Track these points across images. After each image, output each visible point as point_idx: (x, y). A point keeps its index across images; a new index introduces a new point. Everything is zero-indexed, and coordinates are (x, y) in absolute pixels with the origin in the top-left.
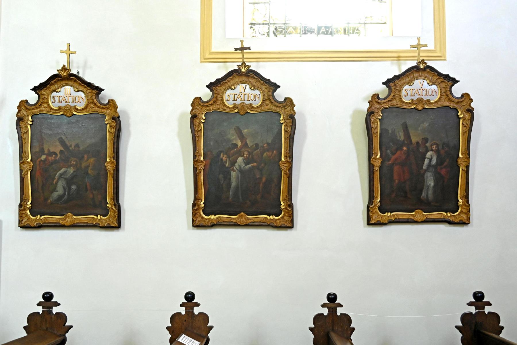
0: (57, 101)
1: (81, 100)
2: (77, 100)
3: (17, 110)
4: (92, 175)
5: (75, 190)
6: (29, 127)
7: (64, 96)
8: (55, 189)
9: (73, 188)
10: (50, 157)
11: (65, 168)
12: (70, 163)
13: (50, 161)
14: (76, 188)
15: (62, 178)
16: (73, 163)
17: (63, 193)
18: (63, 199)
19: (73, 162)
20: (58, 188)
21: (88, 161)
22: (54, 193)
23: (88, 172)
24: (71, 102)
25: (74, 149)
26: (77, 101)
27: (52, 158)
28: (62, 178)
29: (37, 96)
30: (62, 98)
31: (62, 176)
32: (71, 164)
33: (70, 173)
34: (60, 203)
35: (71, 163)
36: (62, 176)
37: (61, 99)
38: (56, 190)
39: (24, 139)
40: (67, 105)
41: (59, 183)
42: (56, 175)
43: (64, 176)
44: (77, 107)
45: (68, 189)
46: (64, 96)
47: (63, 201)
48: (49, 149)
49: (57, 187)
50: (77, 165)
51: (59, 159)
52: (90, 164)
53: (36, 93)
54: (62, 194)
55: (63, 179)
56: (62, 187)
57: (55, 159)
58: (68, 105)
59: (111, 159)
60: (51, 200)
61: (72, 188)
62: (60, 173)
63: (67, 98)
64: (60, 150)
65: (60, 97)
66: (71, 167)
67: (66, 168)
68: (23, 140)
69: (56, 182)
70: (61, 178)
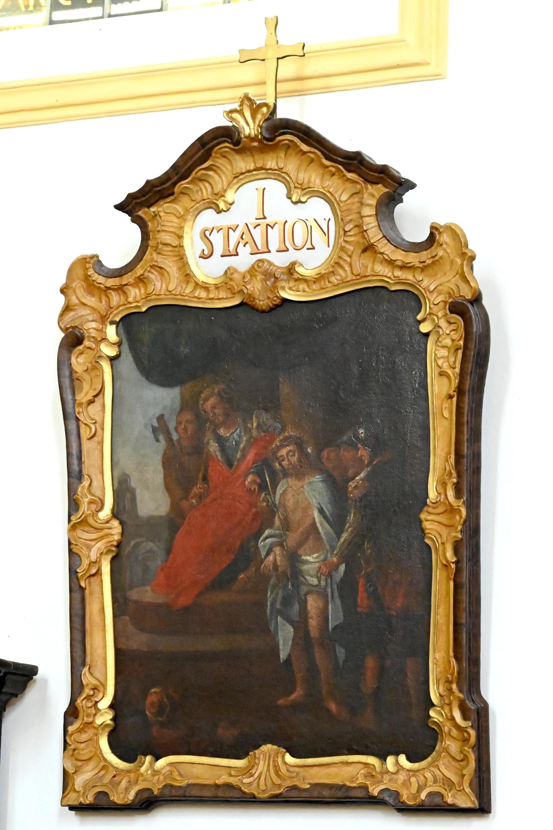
2: (300, 238)
24: (276, 248)
26: (299, 242)
30: (239, 231)
37: (234, 237)
63: (257, 234)
65: (230, 230)
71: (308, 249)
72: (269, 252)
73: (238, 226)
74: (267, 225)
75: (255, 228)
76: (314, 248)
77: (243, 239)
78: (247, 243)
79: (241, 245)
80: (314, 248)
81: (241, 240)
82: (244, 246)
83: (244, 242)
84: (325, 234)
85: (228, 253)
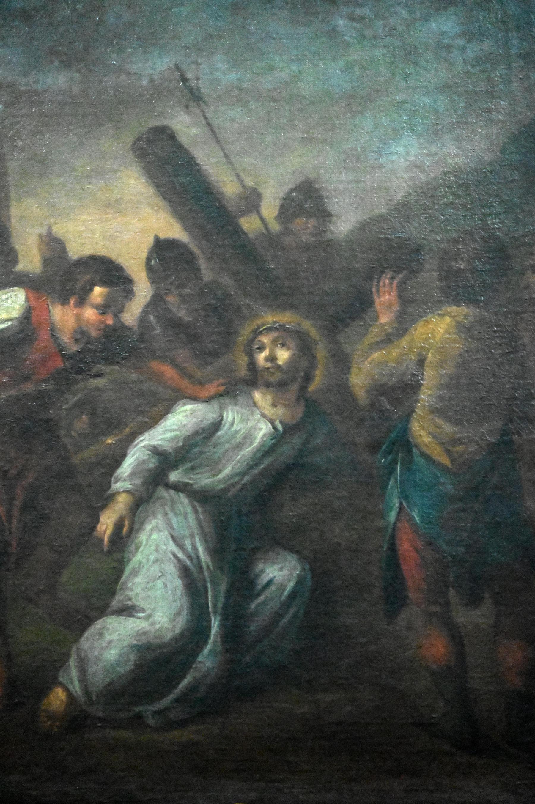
4: (446, 461)
5: (293, 595)
8: (113, 593)
9: (270, 582)
10: (64, 302)
11: (194, 399)
12: (243, 361)
13: (65, 338)
14: (300, 582)
15: (177, 487)
16: (272, 358)
17: (182, 621)
18: (185, 683)
19: (275, 342)
20: (138, 580)
21: (404, 342)
22: (99, 624)
23: (406, 430)
27: (78, 317)
28: (177, 487)
31: (174, 476)
32: (252, 365)
33: (239, 446)
34: (151, 722)
35: (251, 354)
36: (174, 476)
38: (115, 604)
41: (143, 537)
42: (118, 461)
43: (193, 469)
45: (223, 588)
47: (177, 700)
48: (58, 230)
49: (127, 572)
50: (308, 378)
51: (142, 320)
52: (421, 362)
54: (169, 636)
55: (183, 498)
56: (171, 569)
57: (110, 322)
60: (76, 688)
61: (265, 579)
62: (155, 451)
64: (151, 240)
66: (257, 396)
67: (207, 400)
69: (119, 526)
70: (162, 492)
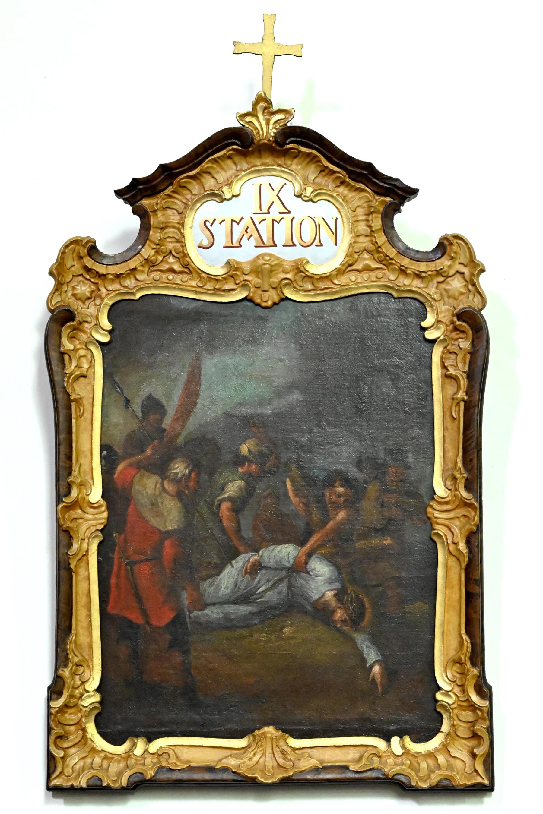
0: (221, 239)
1: (325, 233)
2: (308, 235)
3: (51, 283)
6: (98, 354)
7: (255, 217)
25: (180, 441)
29: (136, 221)
37: (238, 230)
39: (75, 400)
40: (263, 255)
44: (313, 269)
46: (255, 217)
53: (134, 212)
58: (270, 255)
59: (457, 489)
63: (264, 229)
68: (73, 404)
71: (316, 246)
72: (276, 246)
73: (242, 218)
74: (273, 220)
75: (260, 223)
76: (321, 245)
77: (247, 232)
78: (251, 236)
79: (245, 238)
80: (321, 245)
81: (245, 233)
82: (248, 239)
83: (249, 234)
84: (334, 234)
85: (231, 245)
